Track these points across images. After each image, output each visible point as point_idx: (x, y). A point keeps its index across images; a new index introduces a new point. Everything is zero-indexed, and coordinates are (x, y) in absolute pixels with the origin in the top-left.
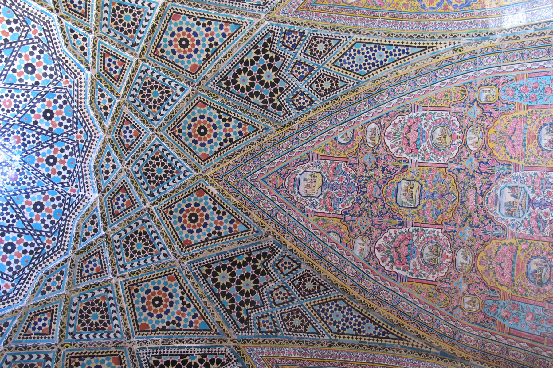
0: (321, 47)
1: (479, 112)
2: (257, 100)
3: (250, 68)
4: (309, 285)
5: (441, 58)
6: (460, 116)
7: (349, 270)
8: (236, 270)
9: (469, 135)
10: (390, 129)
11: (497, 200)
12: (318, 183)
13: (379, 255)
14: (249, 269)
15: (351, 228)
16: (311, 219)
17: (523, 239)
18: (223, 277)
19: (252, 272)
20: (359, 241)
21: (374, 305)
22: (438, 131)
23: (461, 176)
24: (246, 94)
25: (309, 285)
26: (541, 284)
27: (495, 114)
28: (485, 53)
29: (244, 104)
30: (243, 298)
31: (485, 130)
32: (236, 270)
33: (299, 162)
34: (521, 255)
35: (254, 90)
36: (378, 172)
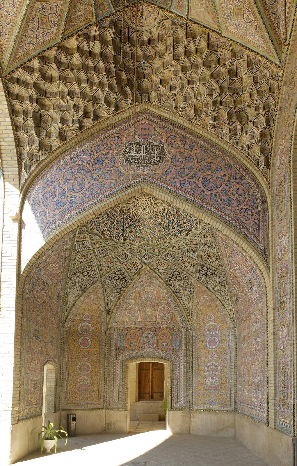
0: (188, 289)
1: (171, 328)
2: (171, 276)
3: (180, 275)
4: (119, 291)
5: (186, 318)
6: (170, 323)
7: (125, 300)
8: (121, 275)
9: (165, 326)
10: (166, 306)
11: (149, 333)
12: (148, 291)
13: (131, 306)
14: (121, 278)
15: (137, 299)
16: (138, 290)
17: (140, 341)
18: (118, 273)
19: (121, 278)
20: (134, 301)
21: (116, 306)
22: (166, 318)
23: (154, 324)
24: (173, 273)
25: (119, 291)
26: (130, 345)
27: (171, 332)
28: (187, 328)
29: (170, 274)
30: (113, 278)
31: (167, 329)
32: (121, 275)
33: (154, 286)
34: (136, 340)
35: (174, 275)
36: (154, 304)
